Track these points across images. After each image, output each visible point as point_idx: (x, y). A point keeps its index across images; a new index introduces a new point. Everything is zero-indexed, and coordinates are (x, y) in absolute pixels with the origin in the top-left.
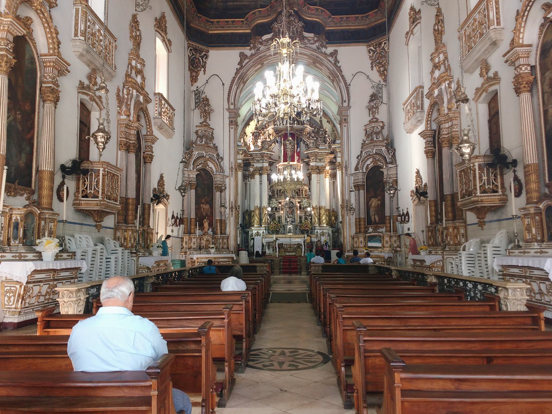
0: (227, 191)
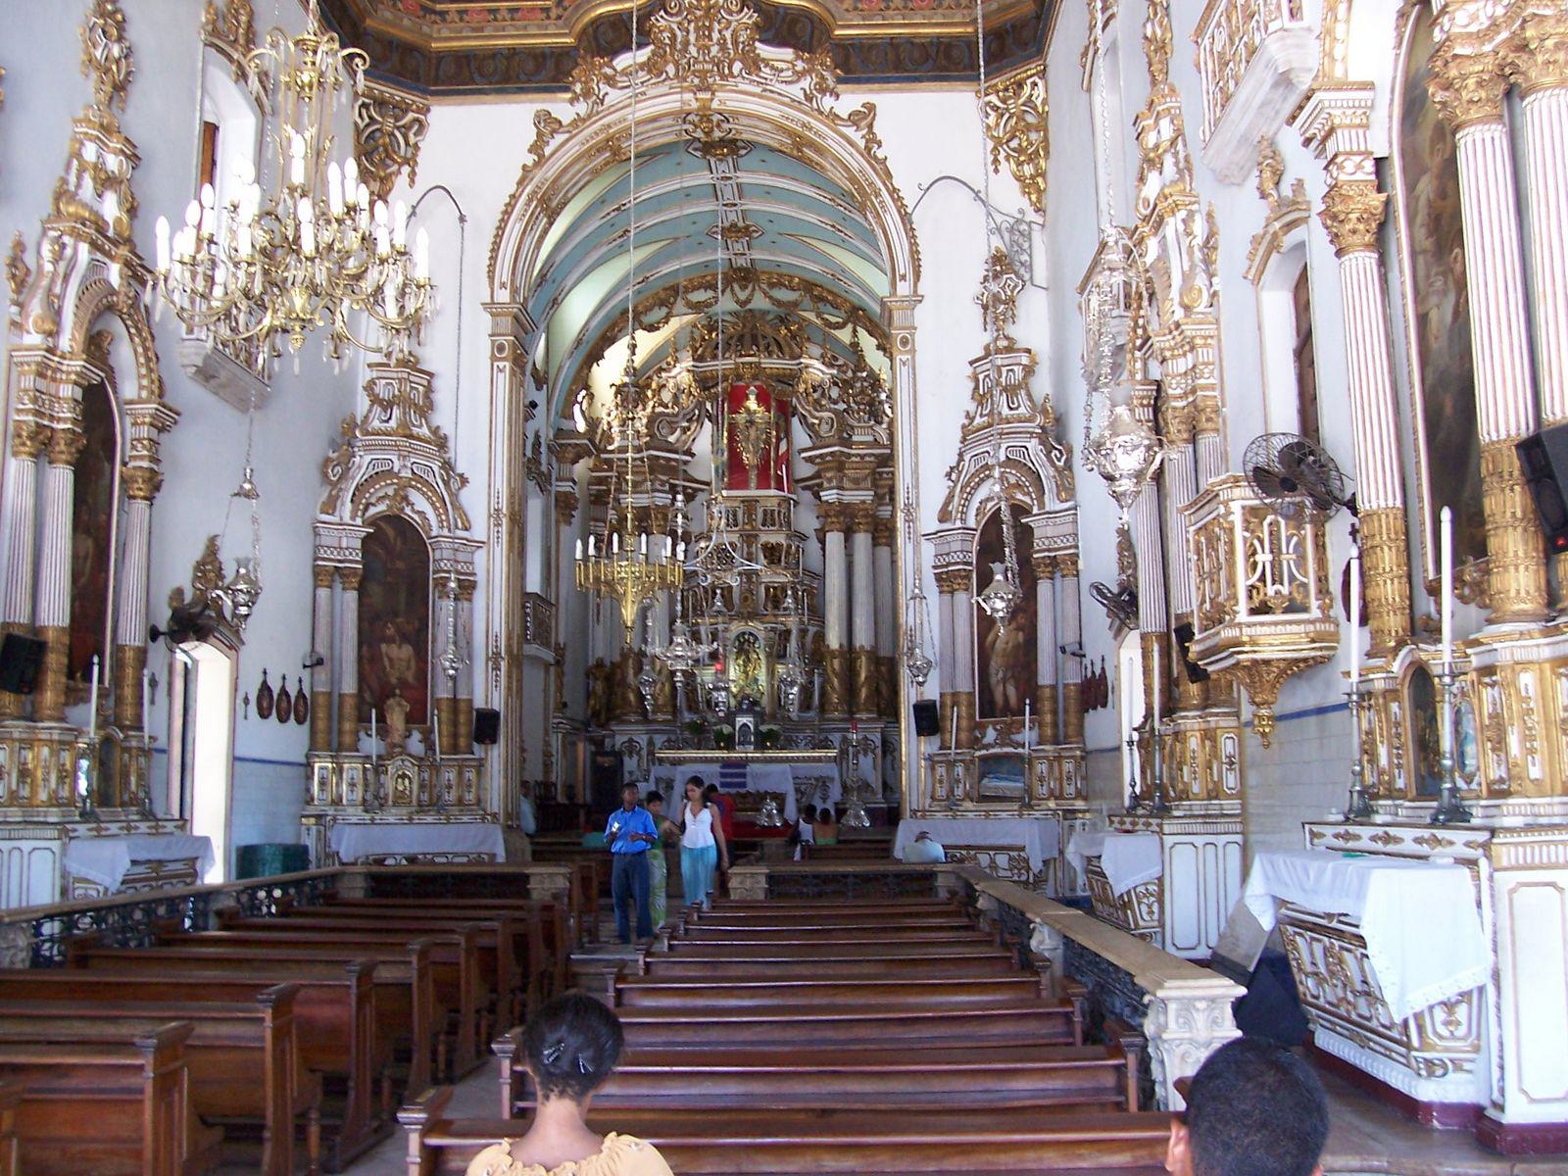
0: (479, 596)
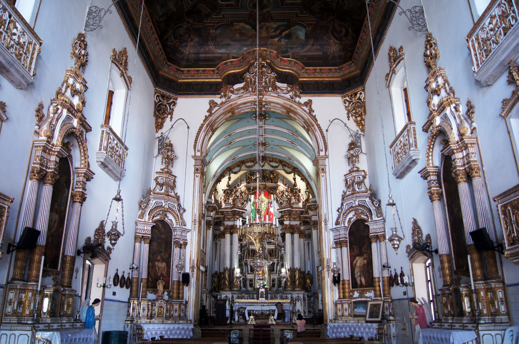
0: (188, 247)
